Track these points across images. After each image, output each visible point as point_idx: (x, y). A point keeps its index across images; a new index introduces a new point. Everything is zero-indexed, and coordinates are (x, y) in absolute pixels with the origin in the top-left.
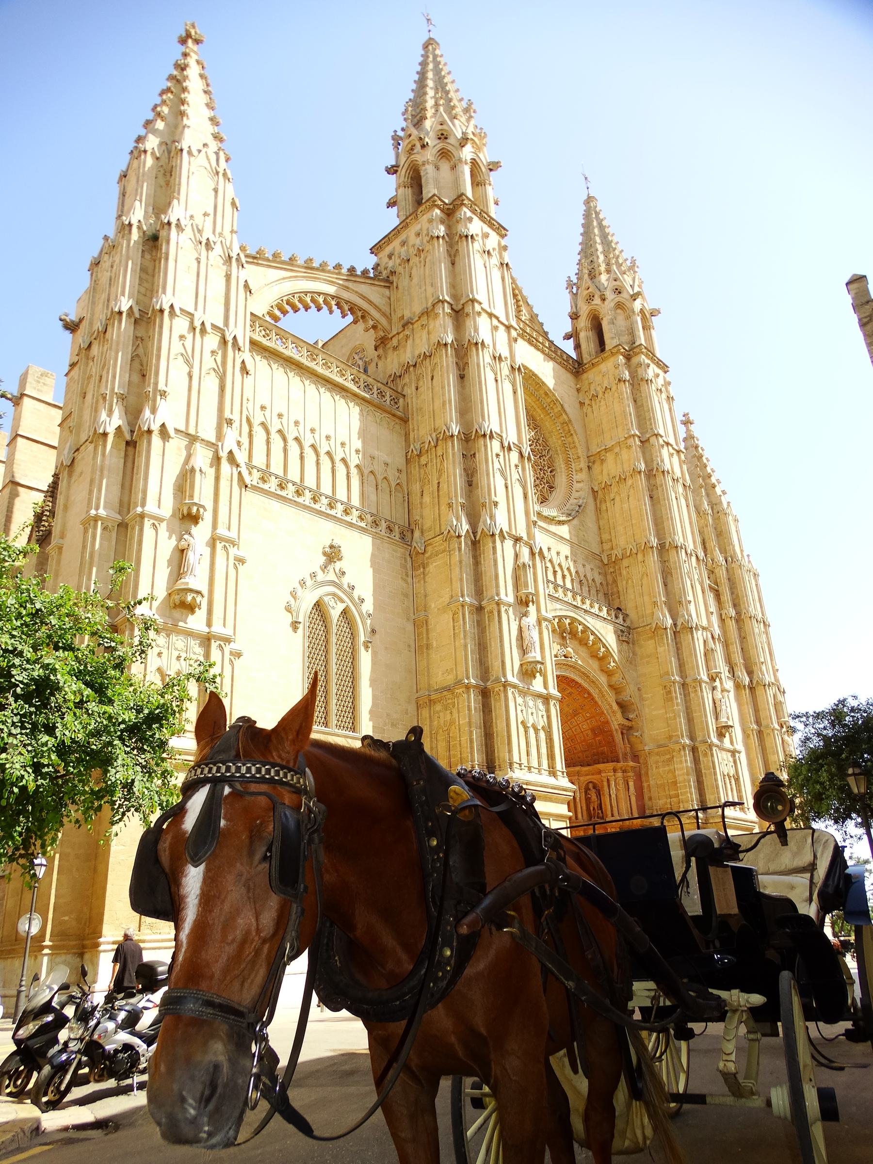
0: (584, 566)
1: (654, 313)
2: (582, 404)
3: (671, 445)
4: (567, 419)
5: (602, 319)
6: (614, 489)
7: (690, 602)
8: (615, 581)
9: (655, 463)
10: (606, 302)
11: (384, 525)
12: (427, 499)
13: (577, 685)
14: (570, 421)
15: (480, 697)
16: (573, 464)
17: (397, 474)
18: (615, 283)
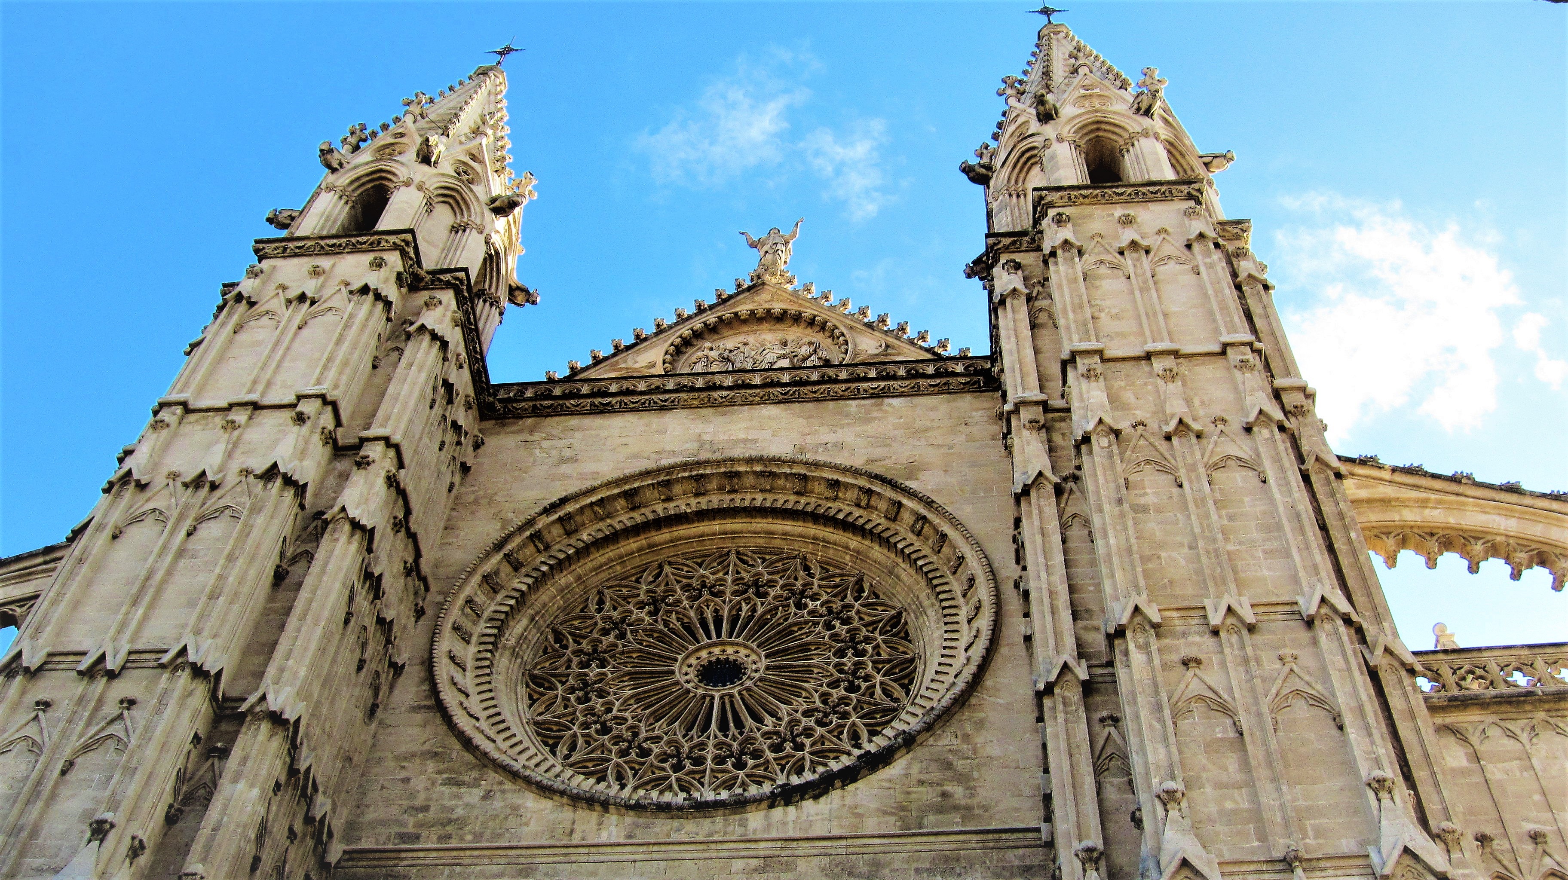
3: (1176, 354)
7: (1168, 798)
14: (929, 503)
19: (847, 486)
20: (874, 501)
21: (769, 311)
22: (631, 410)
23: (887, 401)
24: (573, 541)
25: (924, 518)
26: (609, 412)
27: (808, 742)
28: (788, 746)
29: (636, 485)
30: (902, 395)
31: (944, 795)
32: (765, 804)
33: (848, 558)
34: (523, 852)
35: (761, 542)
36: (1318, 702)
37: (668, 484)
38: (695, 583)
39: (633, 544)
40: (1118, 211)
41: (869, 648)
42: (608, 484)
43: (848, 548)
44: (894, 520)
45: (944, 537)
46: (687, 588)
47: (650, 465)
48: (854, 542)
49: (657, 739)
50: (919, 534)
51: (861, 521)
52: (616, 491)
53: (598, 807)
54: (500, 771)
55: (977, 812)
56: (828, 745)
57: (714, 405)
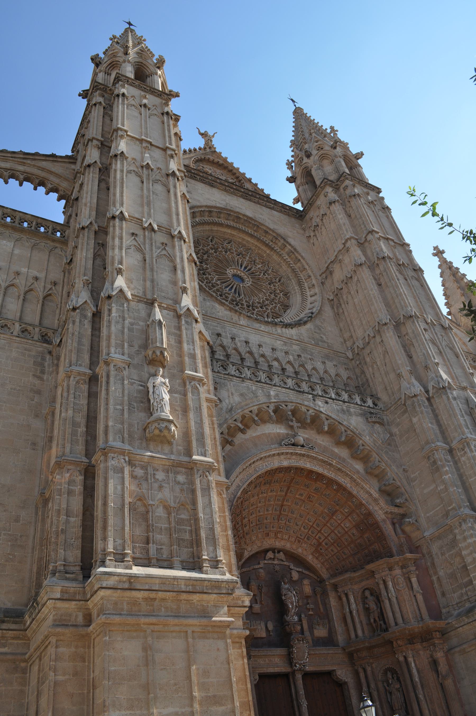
0: (324, 363)
1: (360, 155)
3: (393, 240)
4: (292, 249)
5: (311, 170)
6: (345, 291)
9: (375, 254)
10: (312, 158)
13: (320, 477)
14: (295, 249)
16: (306, 284)
19: (270, 234)
20: (277, 242)
21: (218, 162)
22: (203, 183)
23: (273, 211)
24: (194, 220)
25: (293, 253)
26: (196, 180)
27: (269, 308)
28: (265, 309)
29: (213, 209)
30: (277, 211)
31: (321, 337)
32: (281, 326)
33: (265, 255)
34: (222, 321)
35: (240, 241)
36: (451, 349)
37: (220, 213)
38: (224, 246)
39: (207, 228)
40: (365, 190)
41: (277, 285)
42: (206, 206)
43: (266, 252)
45: (299, 260)
46: (223, 248)
47: (213, 204)
48: (268, 252)
49: (229, 294)
50: (290, 257)
51: (273, 246)
52: (207, 209)
53: (238, 313)
54: (206, 293)
55: (330, 345)
56: (273, 311)
57: (225, 190)
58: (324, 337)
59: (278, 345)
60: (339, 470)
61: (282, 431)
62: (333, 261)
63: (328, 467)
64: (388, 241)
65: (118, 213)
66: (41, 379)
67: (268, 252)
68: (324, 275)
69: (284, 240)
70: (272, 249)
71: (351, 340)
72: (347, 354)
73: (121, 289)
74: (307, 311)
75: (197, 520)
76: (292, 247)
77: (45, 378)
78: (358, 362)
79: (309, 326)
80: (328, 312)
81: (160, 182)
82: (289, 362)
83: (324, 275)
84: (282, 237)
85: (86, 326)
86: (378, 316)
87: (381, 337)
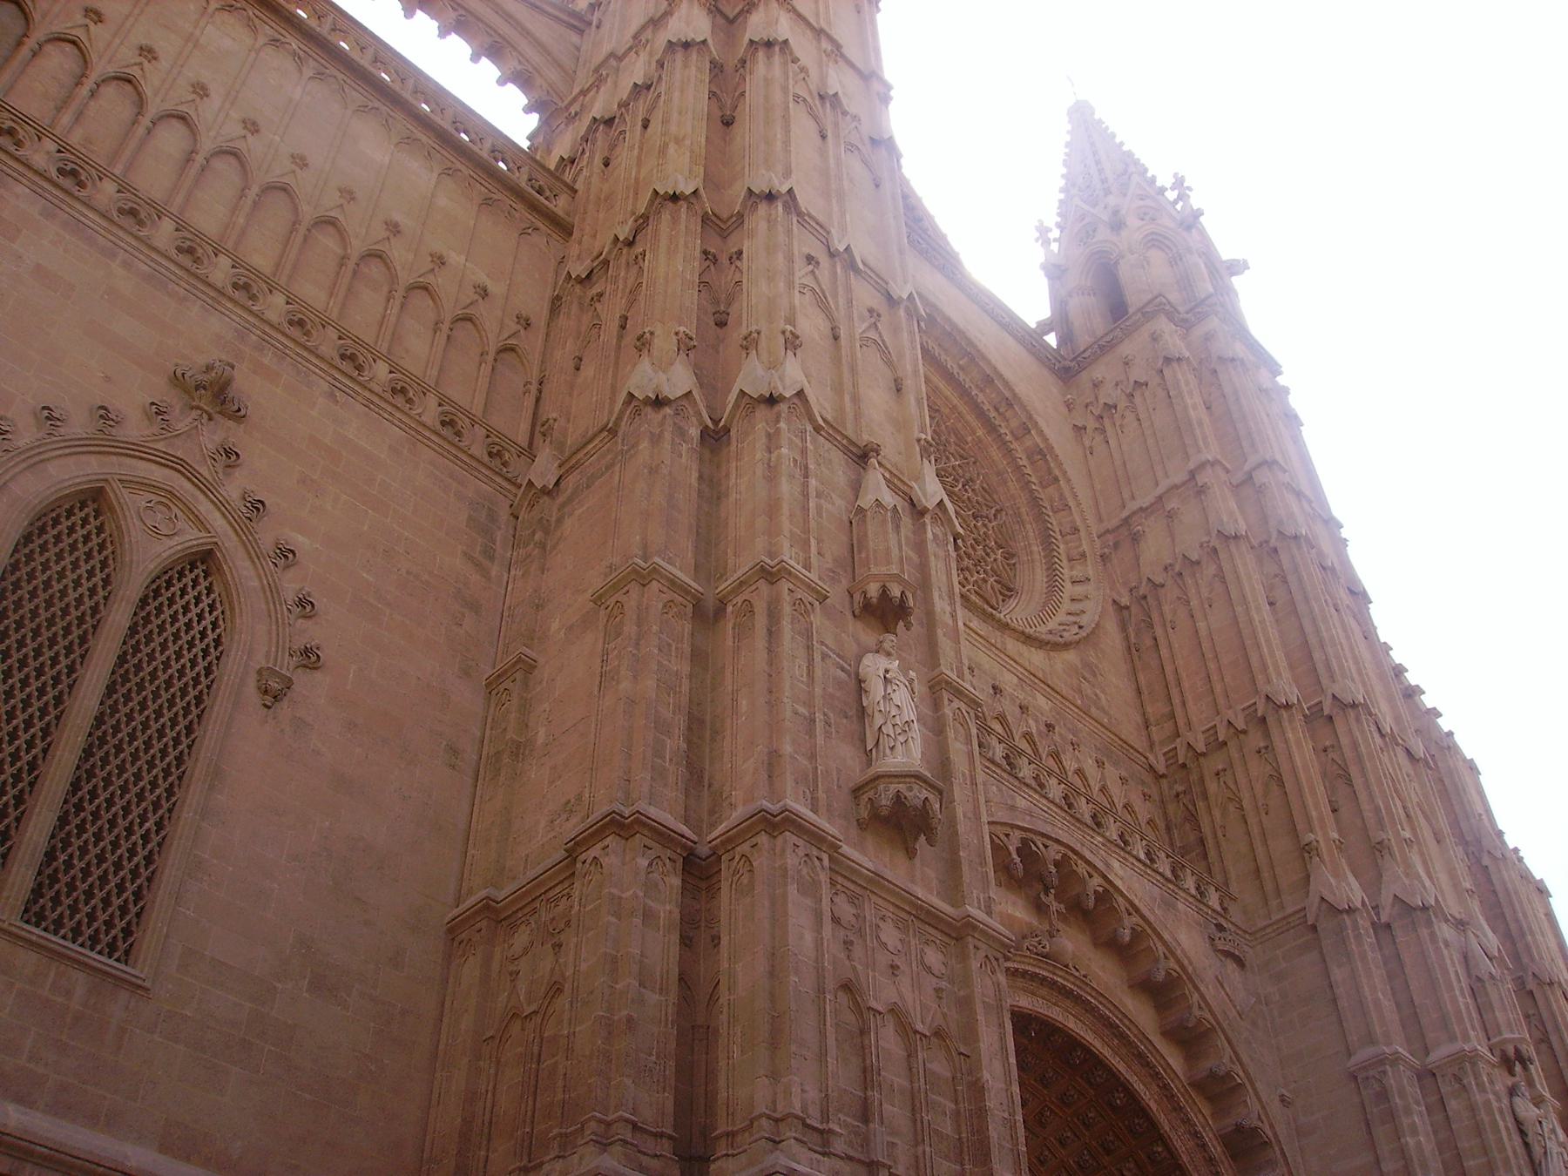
0: (1100, 764)
1: (1237, 267)
2: (1079, 430)
4: (1042, 446)
5: (1117, 263)
7: (1409, 842)
8: (1192, 818)
10: (1124, 233)
11: (430, 411)
12: (588, 371)
13: (1093, 1061)
15: (676, 881)
16: (1062, 546)
17: (513, 326)
18: (1141, 203)
31: (1096, 695)
44: (1017, 439)
45: (1056, 479)
48: (980, 433)
50: (1033, 463)
51: (997, 422)
58: (1102, 696)
59: (1008, 681)
60: (1140, 1056)
61: (1018, 914)
62: (1147, 508)
63: (1116, 1042)
64: (1300, 501)
65: (784, 189)
66: (485, 573)
67: (980, 433)
68: (1110, 539)
69: (1030, 417)
70: (992, 429)
71: (1169, 726)
72: (1151, 757)
73: (802, 390)
74: (1061, 617)
75: (978, 1089)
76: (1046, 440)
77: (493, 573)
78: (1180, 788)
79: (1071, 656)
80: (1112, 637)
81: (856, 152)
82: (1027, 736)
83: (1110, 539)
84: (1024, 407)
85: (684, 460)
86: (1269, 681)
87: (1267, 734)
